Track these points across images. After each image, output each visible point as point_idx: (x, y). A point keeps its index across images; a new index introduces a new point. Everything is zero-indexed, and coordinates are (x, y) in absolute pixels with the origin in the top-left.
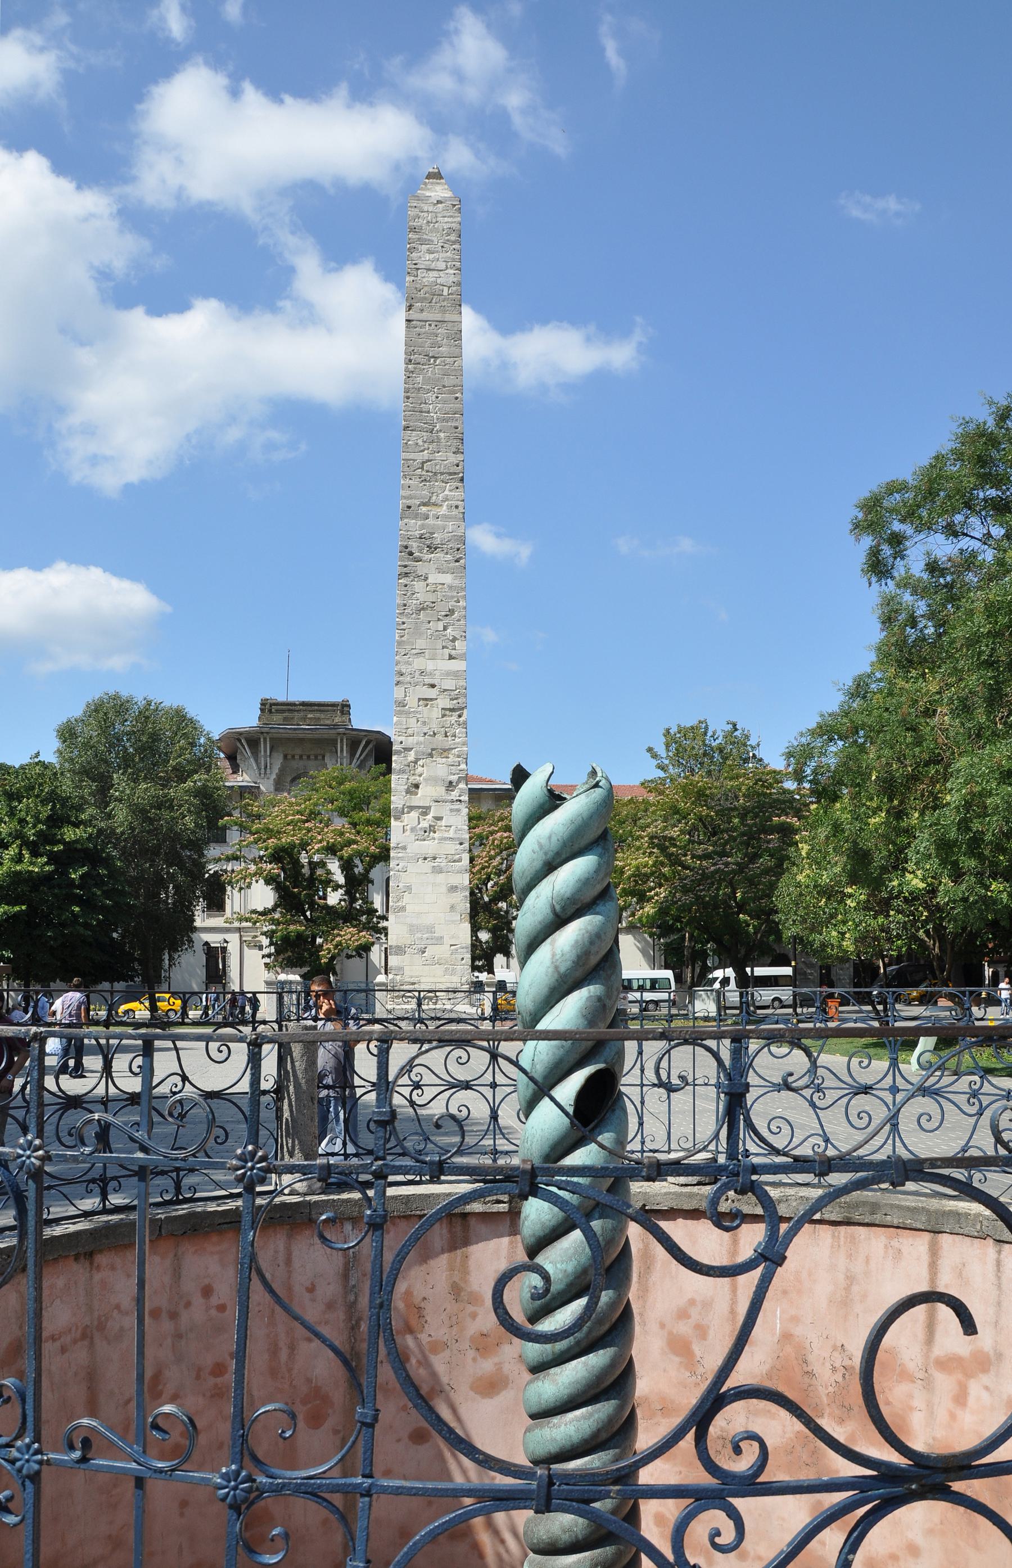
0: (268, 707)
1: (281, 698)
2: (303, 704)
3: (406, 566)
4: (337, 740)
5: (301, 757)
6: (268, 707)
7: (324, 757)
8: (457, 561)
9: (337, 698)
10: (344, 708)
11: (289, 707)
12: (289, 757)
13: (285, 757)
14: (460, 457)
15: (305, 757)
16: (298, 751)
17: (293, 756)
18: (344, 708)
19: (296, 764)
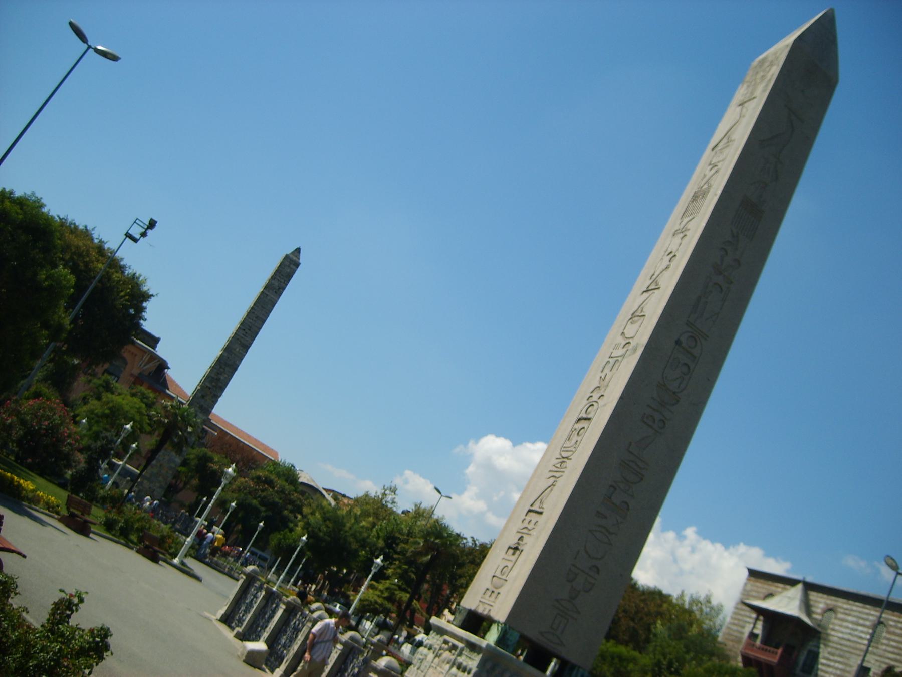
7: (136, 355)
9: (157, 336)
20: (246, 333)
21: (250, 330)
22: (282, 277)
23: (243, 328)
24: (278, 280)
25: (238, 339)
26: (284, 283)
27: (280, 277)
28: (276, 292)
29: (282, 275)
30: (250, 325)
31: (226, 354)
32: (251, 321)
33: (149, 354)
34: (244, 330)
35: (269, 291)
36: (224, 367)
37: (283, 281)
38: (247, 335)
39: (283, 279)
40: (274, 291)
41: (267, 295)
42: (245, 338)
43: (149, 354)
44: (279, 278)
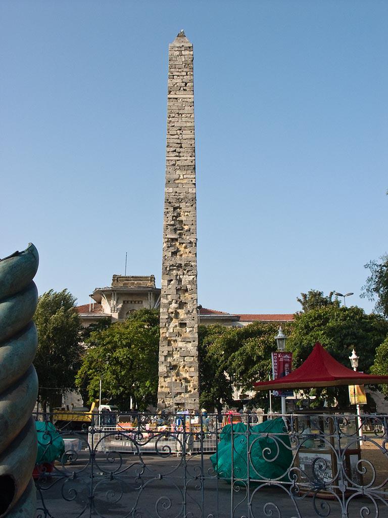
0: (116, 279)
1: (123, 275)
2: (133, 277)
3: (167, 209)
4: (148, 294)
5: (131, 302)
6: (116, 279)
8: (192, 206)
10: (152, 279)
11: (127, 278)
12: (126, 302)
13: (124, 302)
14: (193, 158)
15: (133, 302)
16: (130, 299)
17: (128, 302)
18: (152, 279)
19: (130, 306)
20: (180, 153)
21: (181, 147)
22: (180, 70)
23: (172, 149)
24: (178, 76)
25: (174, 165)
26: (187, 75)
27: (178, 72)
28: (184, 90)
29: (179, 69)
30: (179, 141)
31: (171, 190)
32: (176, 136)
33: (150, 294)
34: (175, 151)
35: (176, 94)
36: (177, 205)
37: (185, 74)
38: (181, 154)
39: (183, 71)
40: (182, 89)
41: (177, 98)
42: (180, 158)
43: (150, 294)
44: (178, 74)
